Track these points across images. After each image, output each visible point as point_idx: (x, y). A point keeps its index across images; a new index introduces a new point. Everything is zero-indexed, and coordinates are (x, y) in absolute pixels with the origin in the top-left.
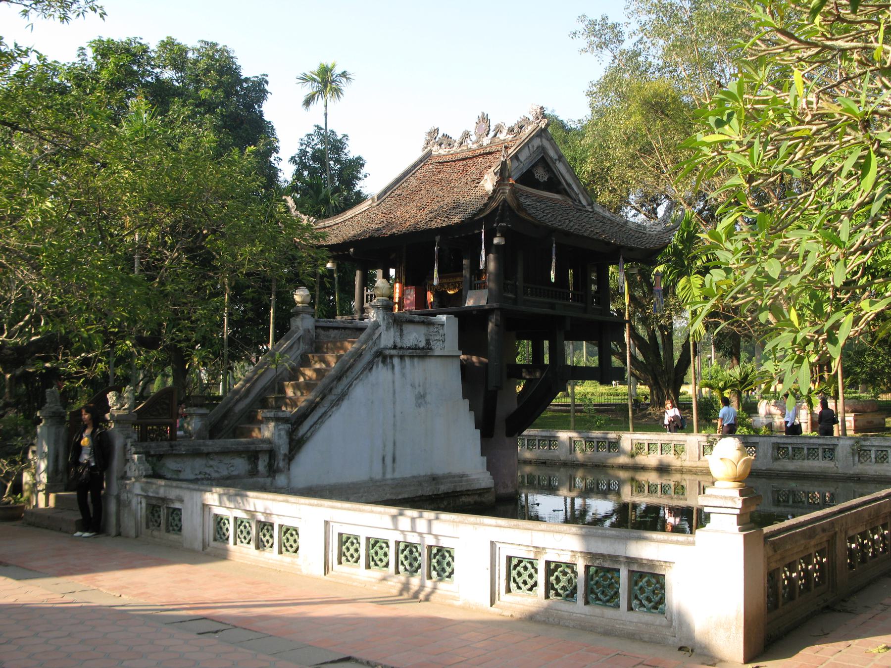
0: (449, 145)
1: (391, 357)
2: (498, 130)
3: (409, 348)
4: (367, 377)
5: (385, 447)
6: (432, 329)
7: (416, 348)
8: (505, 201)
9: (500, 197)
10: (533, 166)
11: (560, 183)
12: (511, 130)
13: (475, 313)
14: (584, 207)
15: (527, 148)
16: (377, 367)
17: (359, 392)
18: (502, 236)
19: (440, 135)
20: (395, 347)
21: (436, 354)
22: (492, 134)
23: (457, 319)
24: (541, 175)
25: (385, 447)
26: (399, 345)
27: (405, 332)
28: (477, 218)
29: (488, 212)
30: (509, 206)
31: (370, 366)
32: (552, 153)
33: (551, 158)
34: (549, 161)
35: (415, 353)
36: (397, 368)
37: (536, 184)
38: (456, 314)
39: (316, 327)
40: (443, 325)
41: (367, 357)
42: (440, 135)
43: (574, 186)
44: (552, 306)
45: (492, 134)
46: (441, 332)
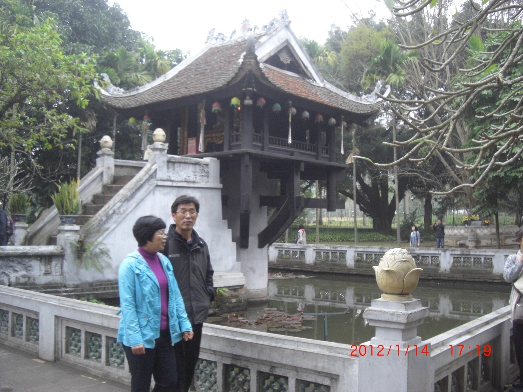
0: (223, 39)
8: (250, 71)
9: (247, 68)
10: (279, 52)
13: (231, 156)
23: (219, 161)
24: (285, 59)
30: (254, 75)
38: (218, 157)
39: (116, 166)
44: (292, 154)
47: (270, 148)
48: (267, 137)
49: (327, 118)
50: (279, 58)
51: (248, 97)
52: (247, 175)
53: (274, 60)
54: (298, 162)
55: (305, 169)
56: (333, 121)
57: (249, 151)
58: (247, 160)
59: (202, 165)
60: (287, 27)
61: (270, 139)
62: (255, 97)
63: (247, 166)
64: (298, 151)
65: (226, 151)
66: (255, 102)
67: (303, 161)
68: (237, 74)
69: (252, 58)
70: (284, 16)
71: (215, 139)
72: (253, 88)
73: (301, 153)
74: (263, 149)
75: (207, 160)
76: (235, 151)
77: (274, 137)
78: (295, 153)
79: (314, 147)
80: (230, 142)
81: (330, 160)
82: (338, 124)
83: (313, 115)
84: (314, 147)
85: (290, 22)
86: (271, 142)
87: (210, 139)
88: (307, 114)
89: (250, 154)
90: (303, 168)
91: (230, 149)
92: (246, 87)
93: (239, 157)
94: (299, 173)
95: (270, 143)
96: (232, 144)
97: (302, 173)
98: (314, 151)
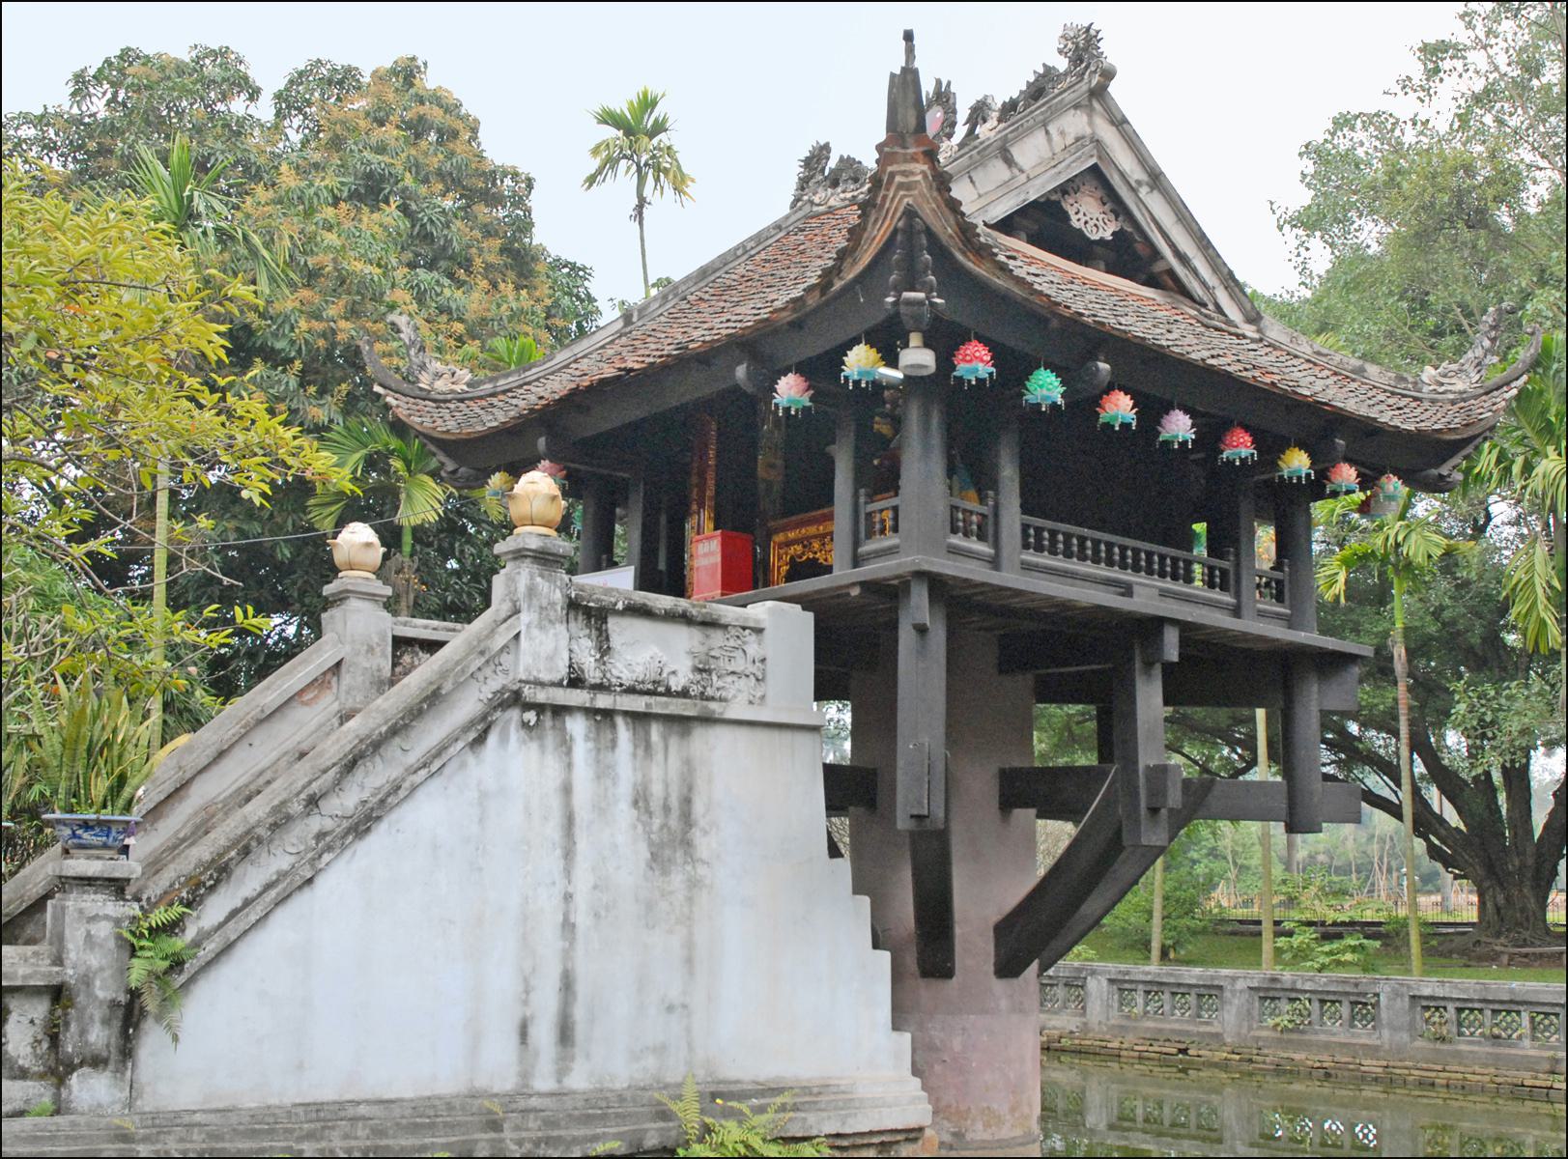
1: (560, 711)
2: (979, 113)
3: (631, 690)
4: (463, 765)
5: (527, 992)
6: (717, 638)
7: (656, 688)
8: (910, 213)
10: (1064, 189)
11: (1156, 254)
12: (1010, 107)
14: (1229, 322)
15: (1040, 135)
16: (504, 739)
17: (427, 813)
18: (926, 345)
19: (832, 163)
20: (576, 681)
21: (730, 714)
22: (961, 131)
23: (810, 616)
24: (1090, 218)
25: (527, 992)
26: (593, 675)
27: (616, 641)
28: (838, 285)
29: (866, 259)
31: (480, 732)
32: (1125, 161)
33: (1122, 175)
34: (1116, 181)
35: (658, 705)
36: (581, 749)
37: (1079, 250)
38: (805, 602)
40: (759, 631)
41: (467, 706)
42: (832, 163)
43: (1199, 263)
44: (1127, 590)
45: (961, 131)
46: (753, 649)
47: (1027, 567)
48: (1012, 517)
49: (1271, 447)
50: (1066, 217)
51: (915, 339)
52: (921, 670)
53: (1043, 222)
54: (1151, 627)
56: (1297, 462)
57: (926, 567)
58: (919, 606)
59: (733, 632)
61: (1025, 527)
62: (945, 339)
63: (921, 630)
64: (1157, 582)
65: (842, 574)
66: (945, 363)
68: (856, 234)
69: (914, 159)
71: (816, 545)
72: (929, 290)
73: (1164, 594)
74: (995, 563)
75: (761, 611)
76: (872, 570)
77: (1039, 522)
78: (1136, 588)
79: (1224, 573)
80: (856, 544)
81: (1291, 622)
82: (1318, 487)
83: (1211, 433)
84: (1224, 573)
85: (1109, 75)
86: (1032, 540)
87: (799, 548)
88: (1179, 427)
89: (937, 585)
90: (1171, 647)
91: (857, 561)
92: (898, 289)
93: (888, 593)
95: (1026, 546)
97: (1168, 669)
98: (1224, 588)
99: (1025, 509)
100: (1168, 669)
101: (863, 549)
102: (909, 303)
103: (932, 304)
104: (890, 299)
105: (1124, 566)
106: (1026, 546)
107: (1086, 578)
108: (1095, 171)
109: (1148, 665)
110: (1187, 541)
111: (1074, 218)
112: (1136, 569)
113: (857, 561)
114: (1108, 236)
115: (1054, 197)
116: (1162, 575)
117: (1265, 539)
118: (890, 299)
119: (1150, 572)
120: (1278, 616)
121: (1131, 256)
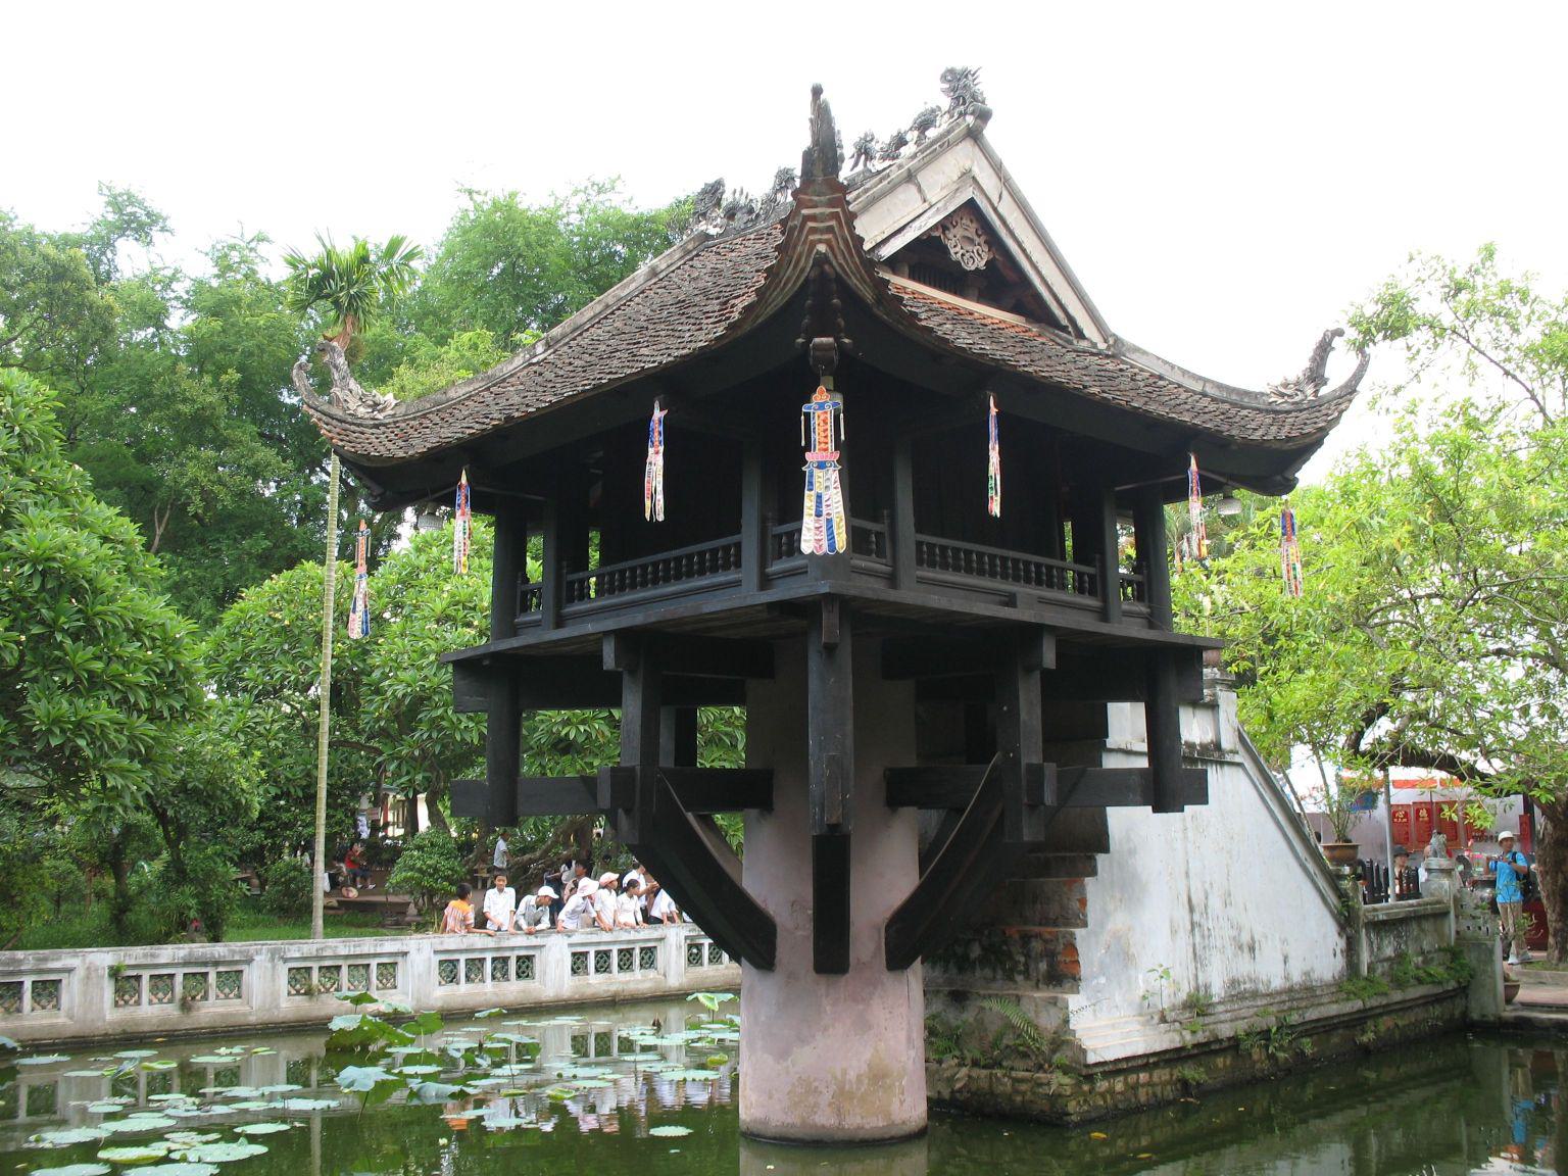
10: (944, 225)
37: (952, 278)
44: (1010, 601)
47: (921, 581)
53: (925, 256)
54: (1032, 633)
55: (1059, 656)
60: (974, 135)
61: (919, 544)
67: (1053, 629)
70: (960, 85)
73: (1042, 601)
78: (1019, 596)
85: (984, 116)
86: (926, 557)
94: (1037, 675)
95: (920, 562)
96: (769, 570)
98: (1092, 593)
99: (919, 529)
100: (1046, 675)
101: (769, 570)
102: (818, 347)
103: (841, 345)
104: (800, 340)
105: (1005, 577)
106: (920, 562)
107: (954, 586)
108: (971, 207)
109: (1029, 670)
110: (1055, 549)
111: (952, 251)
112: (1016, 579)
113: (765, 582)
114: (981, 264)
115: (936, 234)
116: (1039, 583)
117: (1126, 543)
118: (800, 340)
119: (1028, 581)
120: (1139, 615)
121: (1005, 282)
